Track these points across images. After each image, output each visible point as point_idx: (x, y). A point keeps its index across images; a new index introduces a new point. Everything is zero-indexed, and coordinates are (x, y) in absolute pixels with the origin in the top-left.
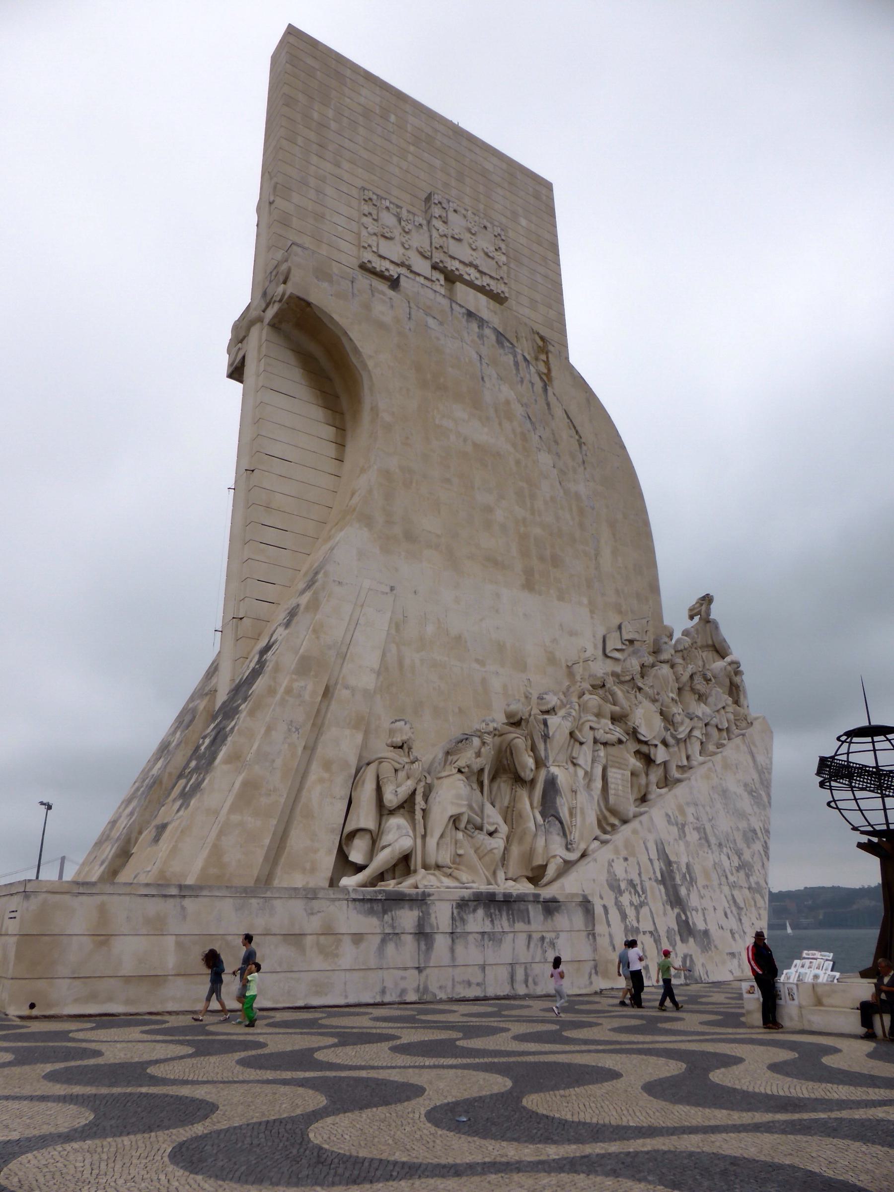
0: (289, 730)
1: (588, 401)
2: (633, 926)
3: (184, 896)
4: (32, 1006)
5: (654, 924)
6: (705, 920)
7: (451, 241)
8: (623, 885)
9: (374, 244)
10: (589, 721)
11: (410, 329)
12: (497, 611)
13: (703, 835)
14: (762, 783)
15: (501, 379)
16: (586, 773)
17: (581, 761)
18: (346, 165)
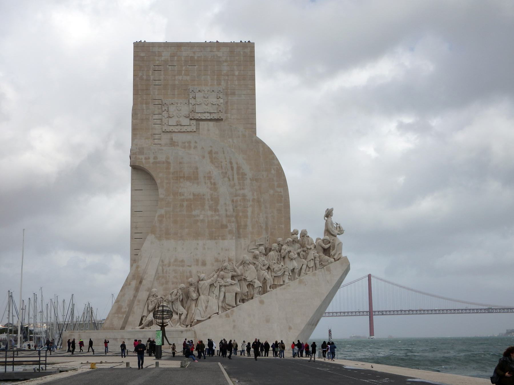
7: (197, 106)
12: (197, 249)
16: (216, 295)
17: (214, 292)
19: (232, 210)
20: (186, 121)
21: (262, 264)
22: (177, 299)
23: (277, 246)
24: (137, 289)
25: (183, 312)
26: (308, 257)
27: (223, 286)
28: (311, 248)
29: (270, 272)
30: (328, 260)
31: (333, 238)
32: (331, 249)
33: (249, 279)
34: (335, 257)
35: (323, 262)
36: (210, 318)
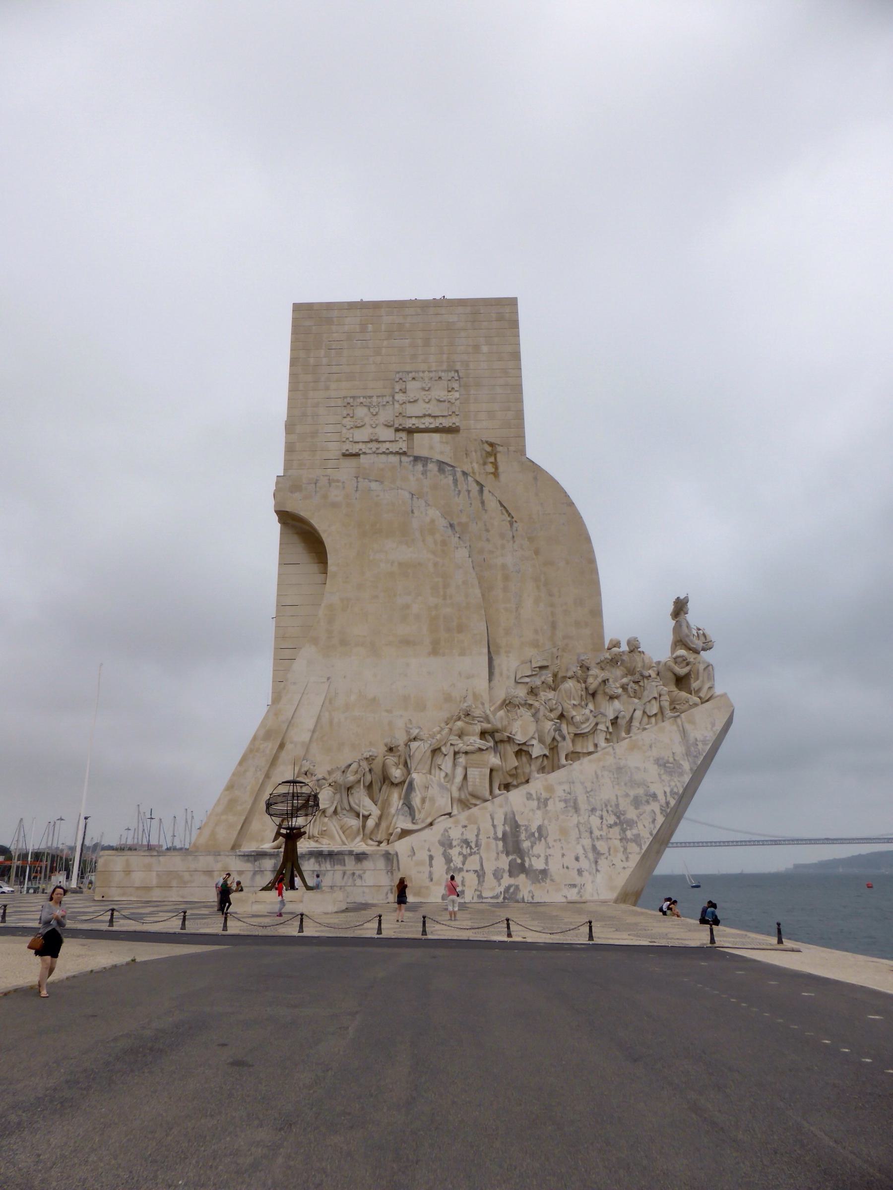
0: (256, 770)
1: (535, 479)
2: (457, 867)
3: (160, 856)
4: (103, 897)
5: (482, 865)
6: (547, 863)
7: (408, 405)
8: (454, 843)
9: (351, 435)
10: (451, 740)
11: (356, 499)
13: (572, 804)
14: (688, 754)
15: (429, 505)
17: (442, 767)
18: (333, 386)
19: (480, 595)
20: (387, 434)
21: (547, 707)
22: (359, 781)
23: (579, 668)
24: (274, 762)
25: (372, 811)
26: (646, 693)
27: (461, 754)
28: (650, 676)
29: (564, 727)
30: (688, 699)
31: (695, 655)
32: (693, 676)
33: (520, 738)
34: (702, 694)
35: (678, 704)
36: (431, 824)
